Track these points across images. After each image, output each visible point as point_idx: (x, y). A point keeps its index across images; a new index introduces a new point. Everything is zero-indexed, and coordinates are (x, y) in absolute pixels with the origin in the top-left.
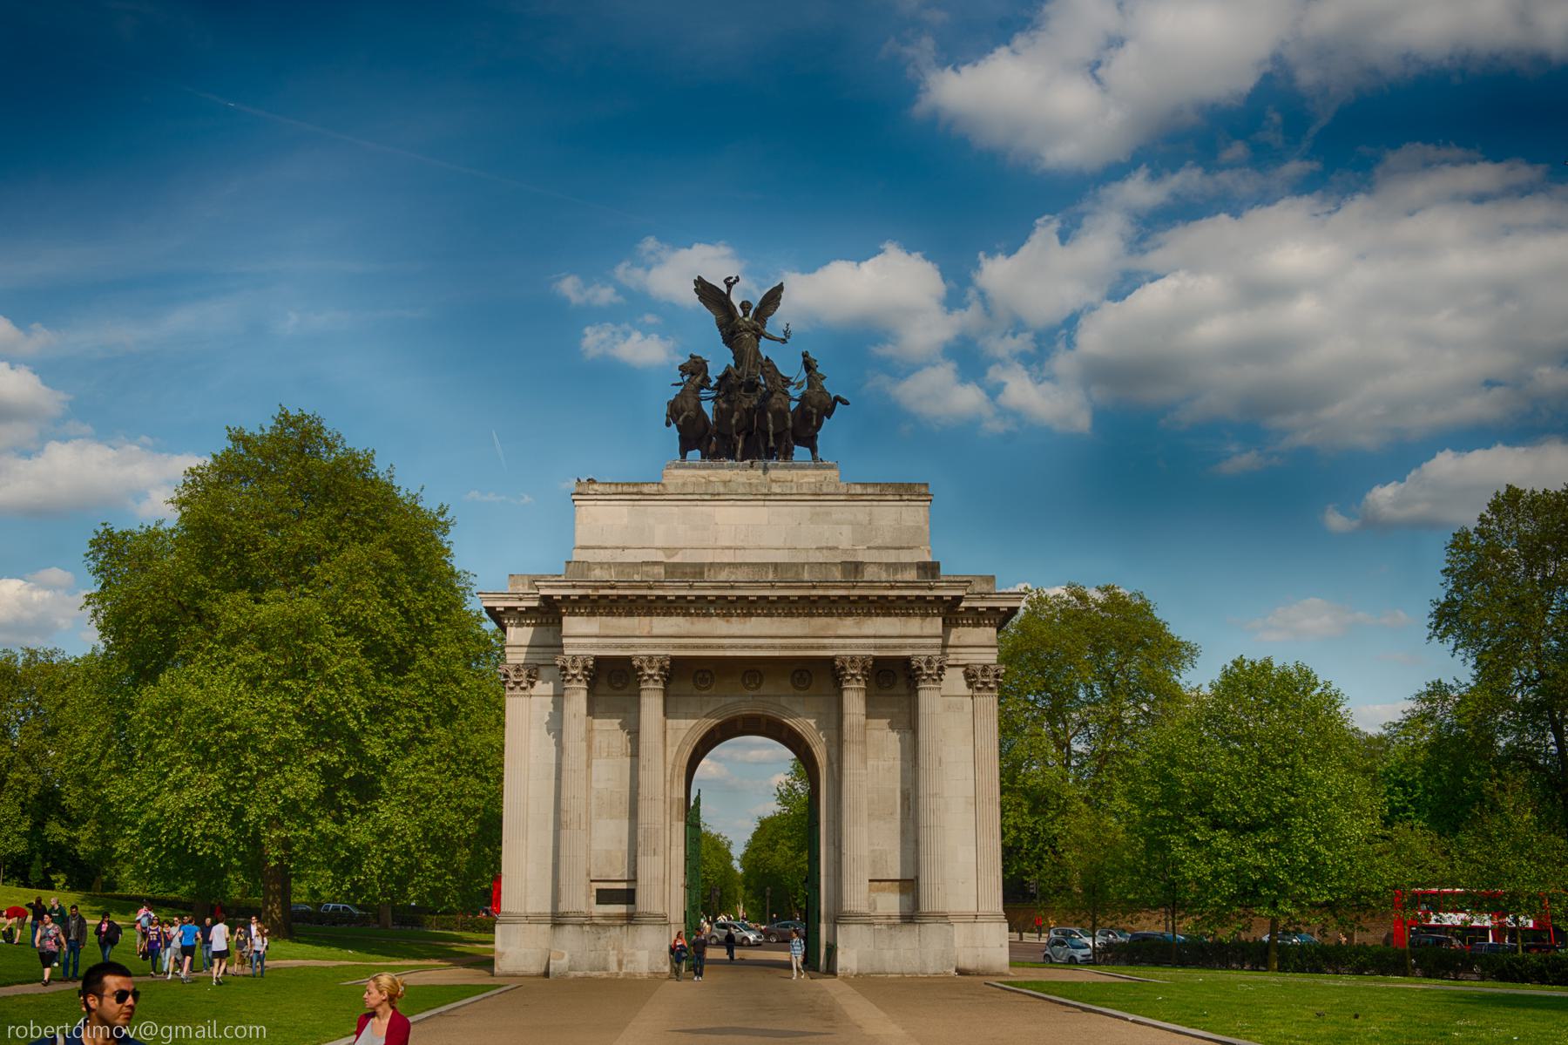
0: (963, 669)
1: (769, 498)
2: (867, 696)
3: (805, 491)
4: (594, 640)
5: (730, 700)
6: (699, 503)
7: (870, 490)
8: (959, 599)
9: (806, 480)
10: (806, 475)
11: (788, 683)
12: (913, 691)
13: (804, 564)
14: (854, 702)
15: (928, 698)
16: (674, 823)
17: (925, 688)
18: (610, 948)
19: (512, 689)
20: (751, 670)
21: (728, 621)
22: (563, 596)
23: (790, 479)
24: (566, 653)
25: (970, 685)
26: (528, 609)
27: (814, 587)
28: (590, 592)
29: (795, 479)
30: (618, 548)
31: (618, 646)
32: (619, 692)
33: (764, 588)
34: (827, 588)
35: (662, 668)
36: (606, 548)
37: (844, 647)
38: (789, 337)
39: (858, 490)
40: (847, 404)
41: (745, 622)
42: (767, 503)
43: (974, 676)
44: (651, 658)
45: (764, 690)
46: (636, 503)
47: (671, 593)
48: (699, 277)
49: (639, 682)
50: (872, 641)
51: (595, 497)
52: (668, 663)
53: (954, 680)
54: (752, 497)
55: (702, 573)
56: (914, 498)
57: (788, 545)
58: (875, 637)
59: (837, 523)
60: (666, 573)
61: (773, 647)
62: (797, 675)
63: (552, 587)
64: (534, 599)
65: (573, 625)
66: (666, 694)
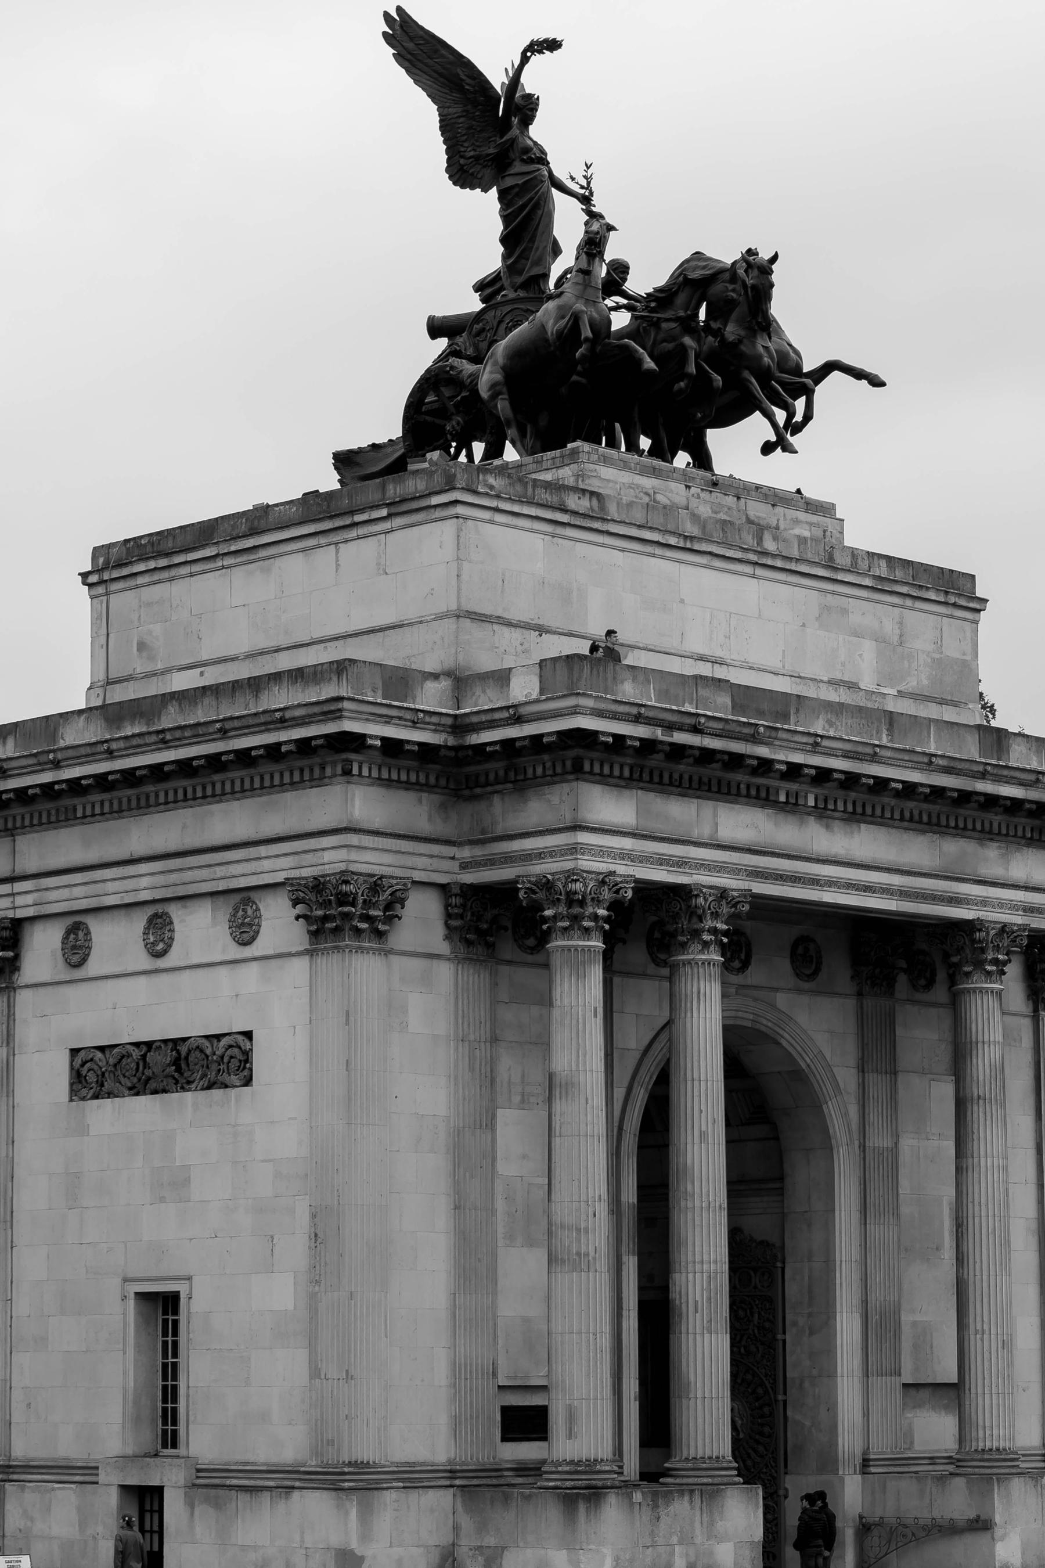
1: (764, 561)
3: (809, 556)
4: (627, 843)
6: (658, 551)
7: (899, 574)
9: (797, 531)
10: (797, 522)
11: (785, 965)
13: (930, 720)
16: (625, 1259)
17: (981, 990)
18: (675, 1540)
19: (358, 932)
21: (828, 827)
22: (615, 736)
23: (774, 524)
27: (983, 776)
28: (659, 734)
29: (782, 526)
30: (527, 626)
31: (662, 861)
32: (530, 958)
33: (917, 766)
34: (998, 779)
36: (509, 624)
37: (984, 902)
38: (591, 194)
39: (882, 570)
40: (876, 382)
41: (852, 833)
42: (760, 571)
44: (723, 894)
45: (755, 975)
46: (560, 530)
47: (780, 756)
48: (399, 10)
50: (1020, 896)
51: (494, 503)
52: (747, 907)
54: (739, 555)
55: (785, 717)
56: (962, 602)
57: (788, 668)
58: (1027, 888)
59: (856, 634)
60: (733, 708)
61: (886, 891)
62: (800, 950)
63: (599, 714)
64: (437, 728)
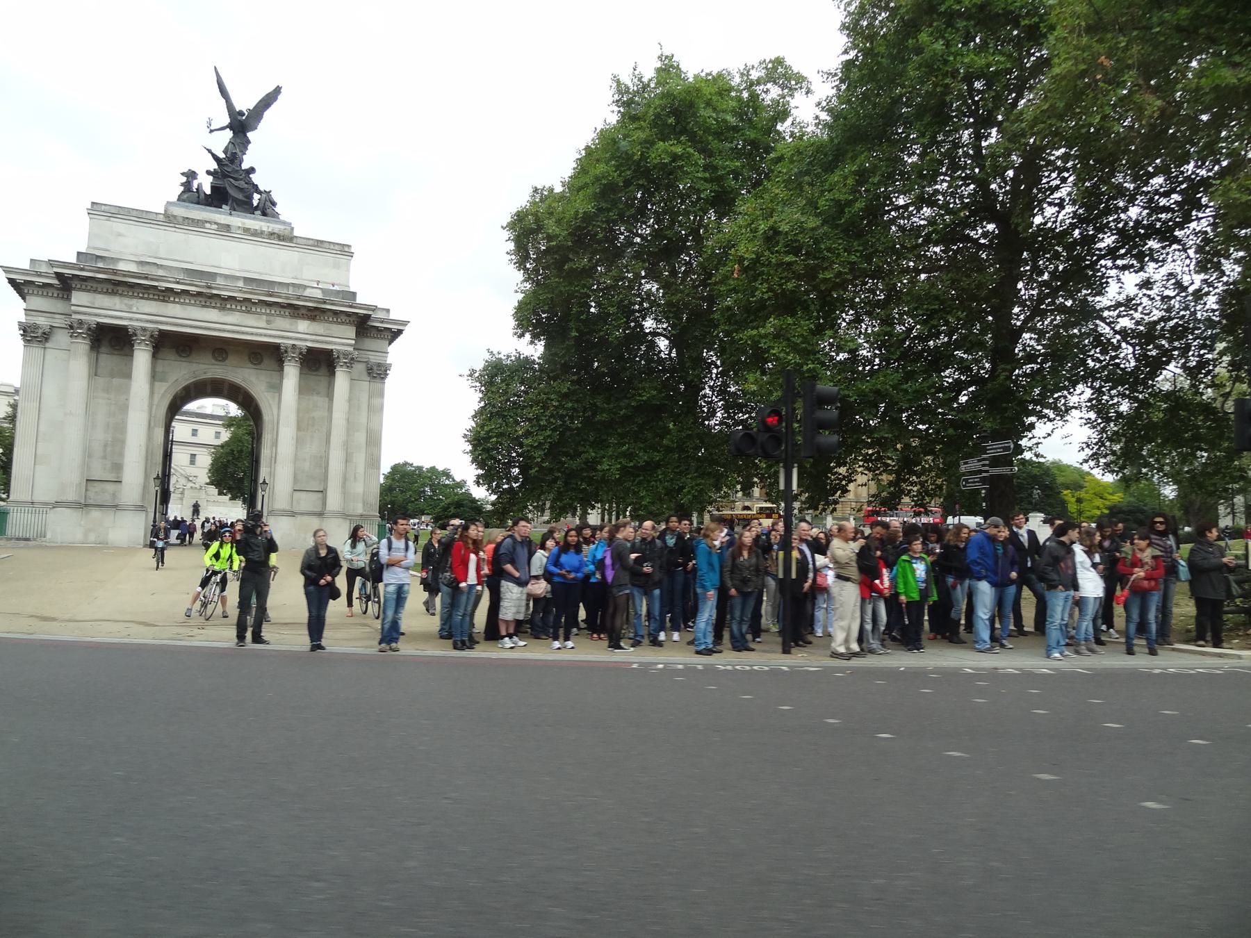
0: (364, 364)
2: (301, 369)
5: (202, 366)
8: (368, 317)
11: (247, 358)
12: (332, 373)
14: (291, 373)
15: (342, 379)
20: (221, 348)
24: (73, 317)
25: (369, 374)
26: (45, 285)
35: (152, 336)
43: (371, 369)
44: (144, 329)
49: (133, 345)
53: (360, 368)
65: (79, 298)
66: (155, 356)
